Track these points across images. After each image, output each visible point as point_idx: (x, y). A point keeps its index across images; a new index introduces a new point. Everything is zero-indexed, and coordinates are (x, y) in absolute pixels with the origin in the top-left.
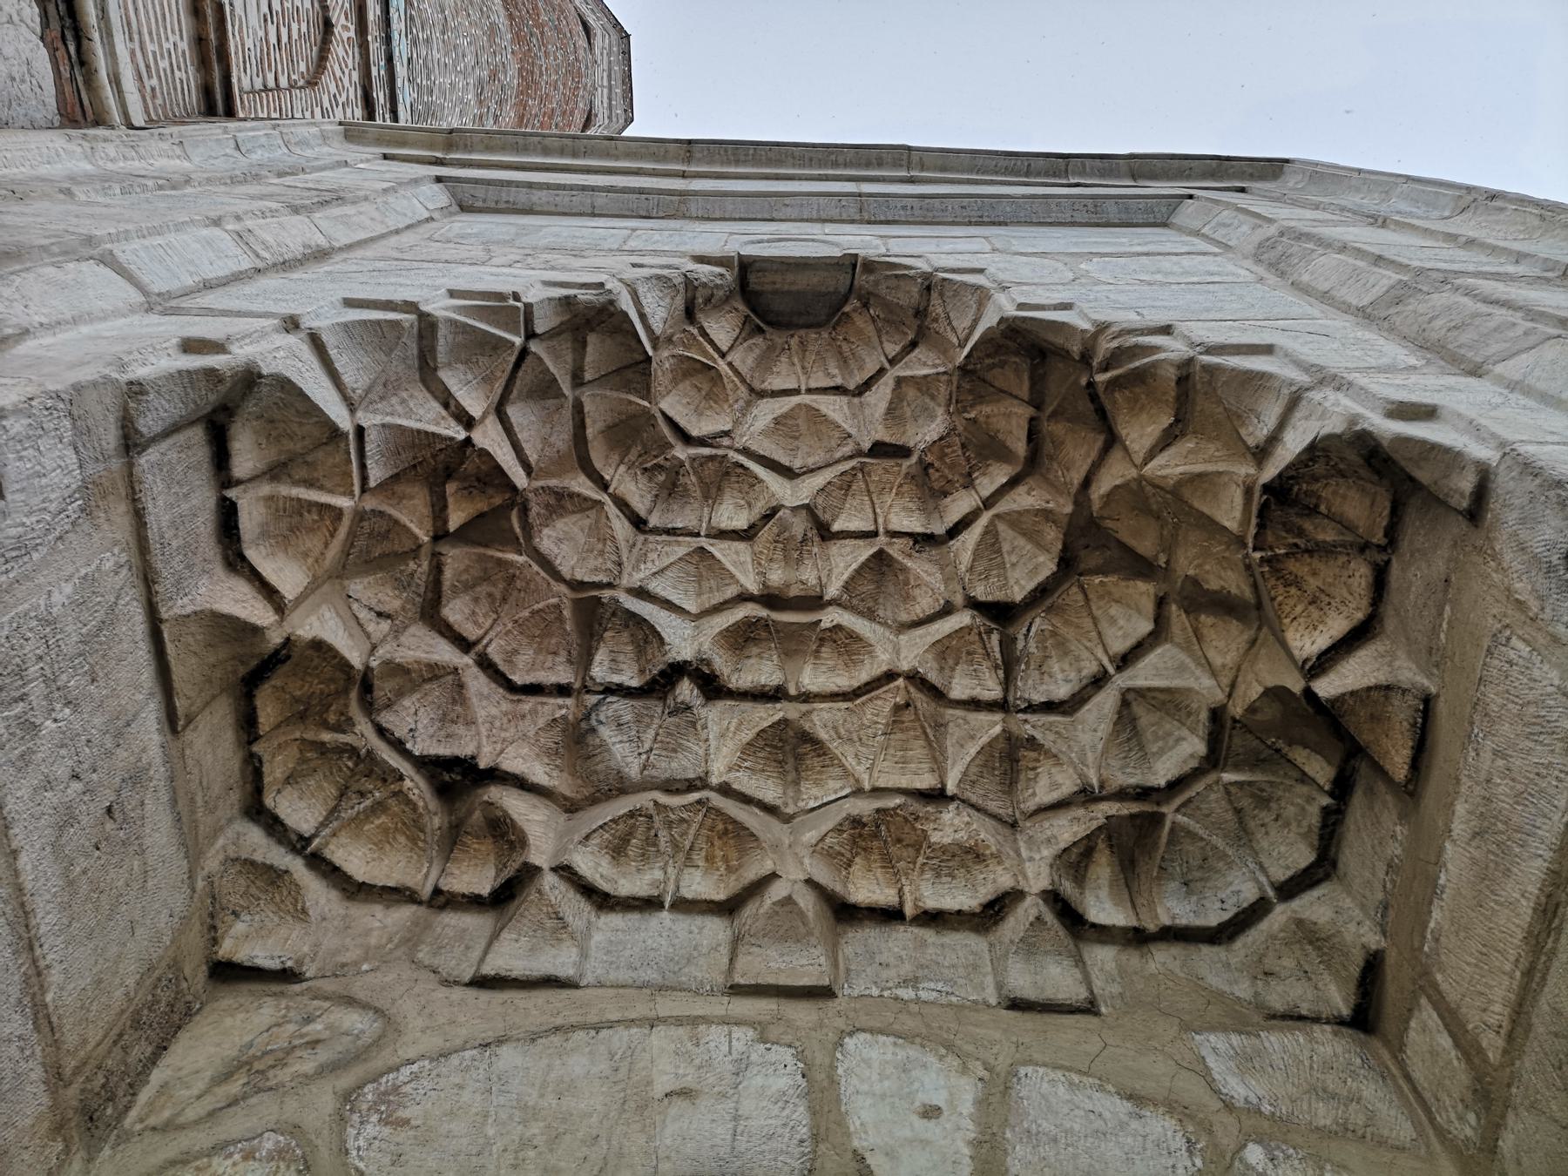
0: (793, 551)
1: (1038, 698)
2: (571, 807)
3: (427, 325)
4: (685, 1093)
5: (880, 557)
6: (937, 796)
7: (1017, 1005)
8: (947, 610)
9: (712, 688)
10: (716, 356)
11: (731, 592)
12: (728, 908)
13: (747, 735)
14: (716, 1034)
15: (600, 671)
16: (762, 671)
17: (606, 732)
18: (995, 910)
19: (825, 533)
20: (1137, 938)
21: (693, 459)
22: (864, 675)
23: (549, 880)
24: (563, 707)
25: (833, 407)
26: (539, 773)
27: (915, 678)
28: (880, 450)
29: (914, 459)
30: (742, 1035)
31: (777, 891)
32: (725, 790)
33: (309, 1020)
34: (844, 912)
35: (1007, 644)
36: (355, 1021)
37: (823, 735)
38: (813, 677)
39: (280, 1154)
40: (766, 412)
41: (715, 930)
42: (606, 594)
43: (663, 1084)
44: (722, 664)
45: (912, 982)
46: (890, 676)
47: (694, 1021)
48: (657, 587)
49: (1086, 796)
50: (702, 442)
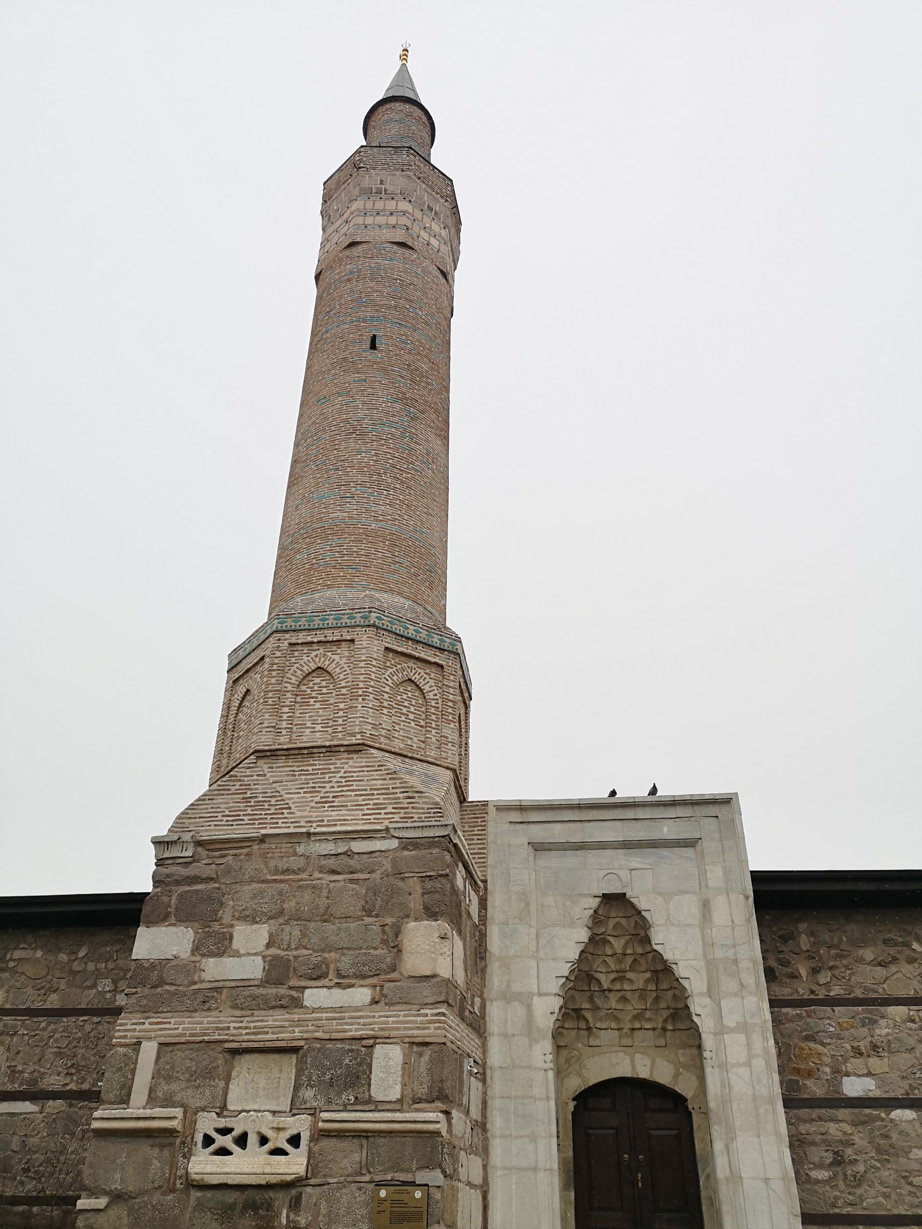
0: (620, 962)
1: (662, 989)
2: (592, 1010)
3: (567, 978)
4: (617, 1064)
5: (635, 959)
6: (646, 1009)
7: (656, 1047)
8: (647, 971)
9: (610, 990)
10: (600, 917)
11: (610, 970)
12: (618, 1029)
13: (617, 998)
14: (619, 1053)
15: (592, 988)
16: (618, 986)
17: (596, 999)
18: (654, 1029)
19: (625, 955)
20: (674, 1030)
21: (600, 939)
22: (634, 989)
23: (594, 1029)
24: (588, 994)
25: (623, 921)
26: (587, 1006)
27: (642, 990)
28: (633, 935)
29: (639, 937)
30: (623, 1053)
31: (625, 1031)
32: (615, 1009)
33: (571, 1053)
34: (633, 1029)
35: (658, 979)
36: (576, 1052)
37: (628, 998)
38: (626, 986)
39: (576, 1074)
40: (612, 923)
41: (616, 1031)
42: (590, 973)
43: (614, 1063)
44: (611, 987)
45: (643, 1042)
46: (638, 989)
47: (617, 1051)
48: (599, 970)
49: (668, 1008)
50: (601, 935)
